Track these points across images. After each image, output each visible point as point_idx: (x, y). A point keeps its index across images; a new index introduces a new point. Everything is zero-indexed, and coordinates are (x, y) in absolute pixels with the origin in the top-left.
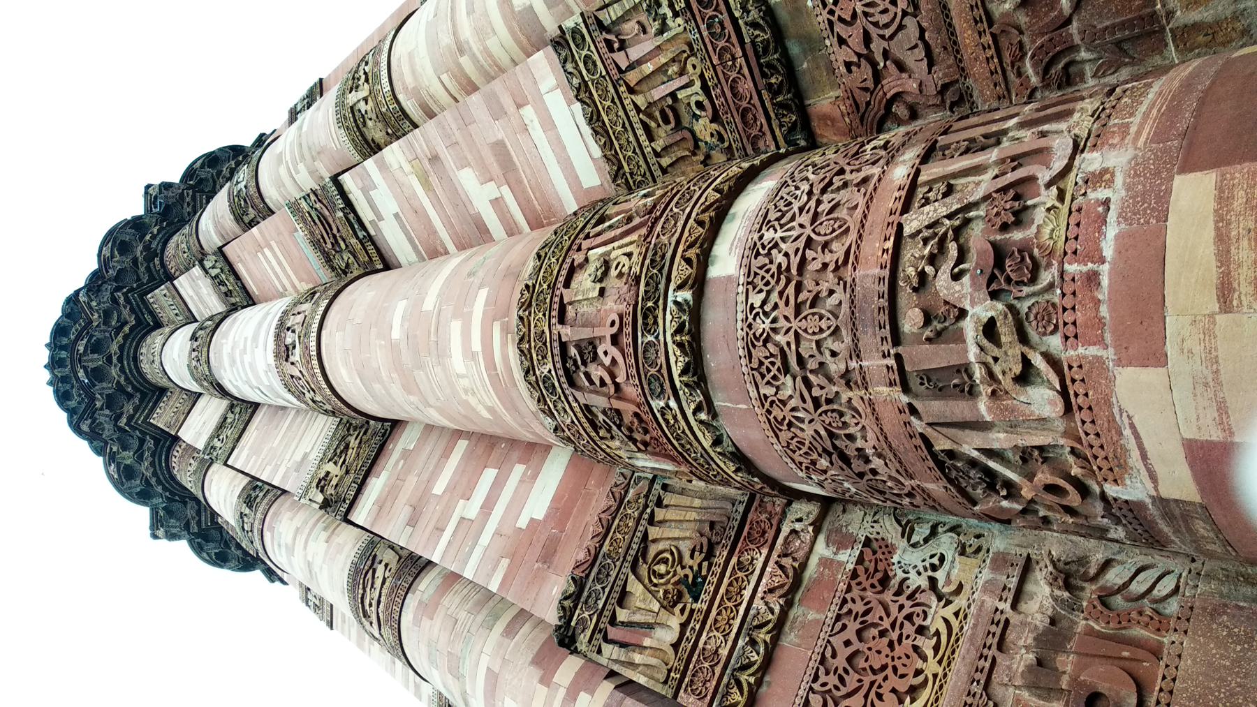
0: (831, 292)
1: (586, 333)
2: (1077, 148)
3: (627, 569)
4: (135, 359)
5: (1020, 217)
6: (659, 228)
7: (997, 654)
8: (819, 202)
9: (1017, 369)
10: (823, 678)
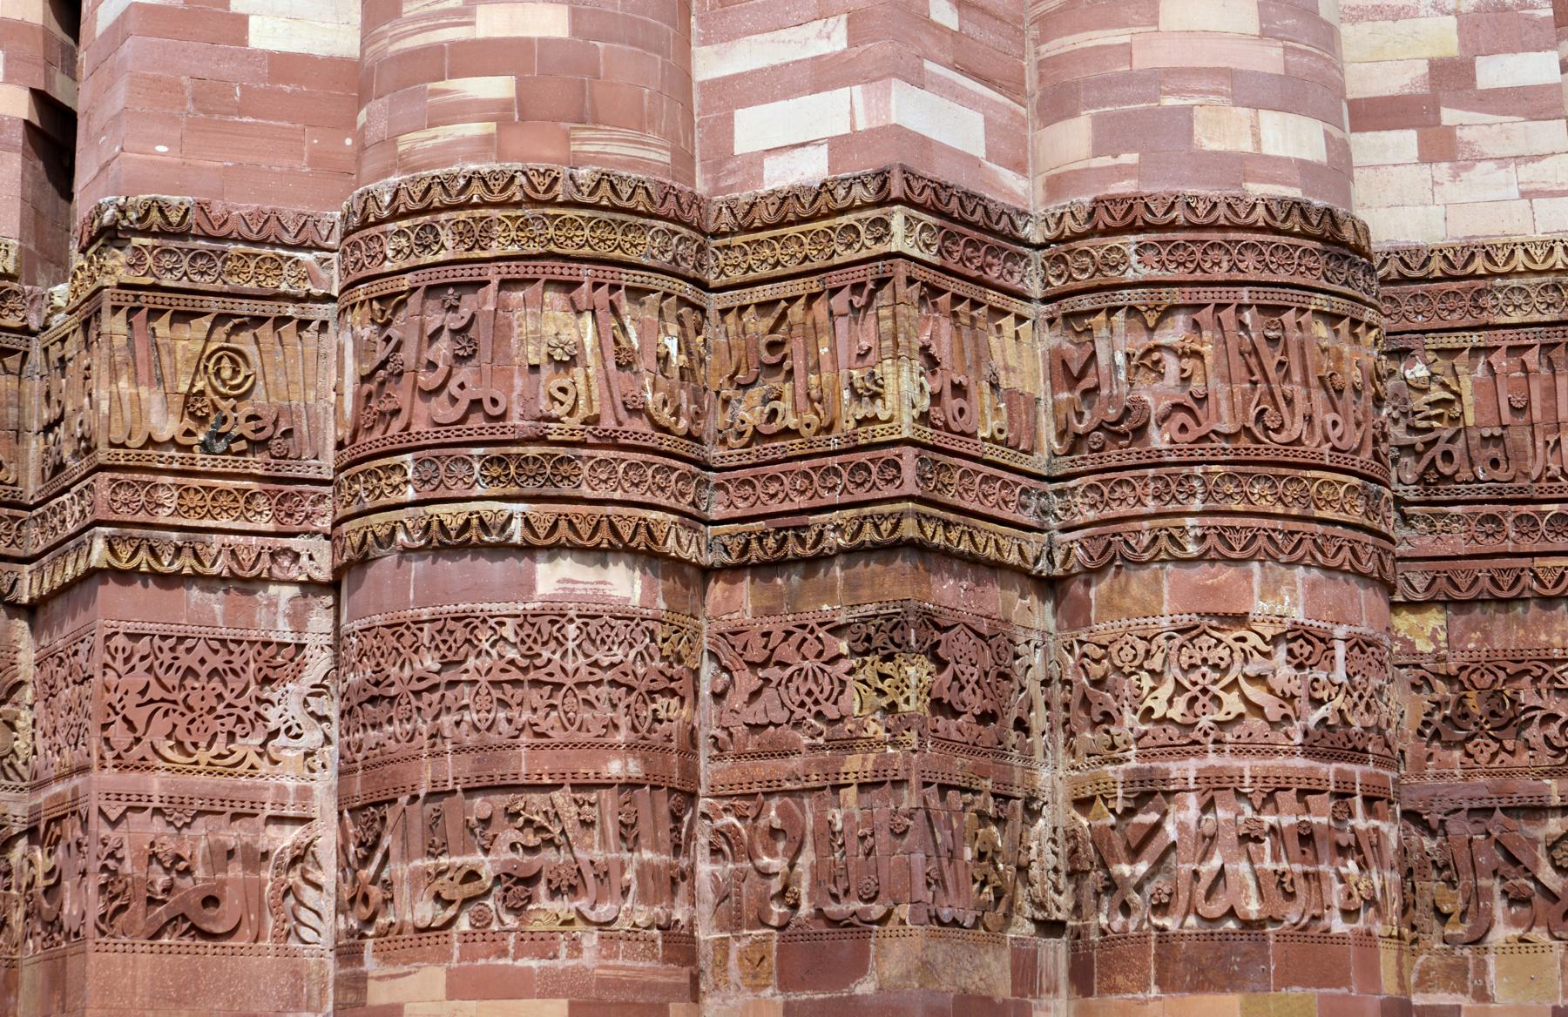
0: (510, 721)
3: (215, 306)
5: (555, 893)
6: (601, 454)
7: (228, 815)
8: (598, 683)
9: (445, 895)
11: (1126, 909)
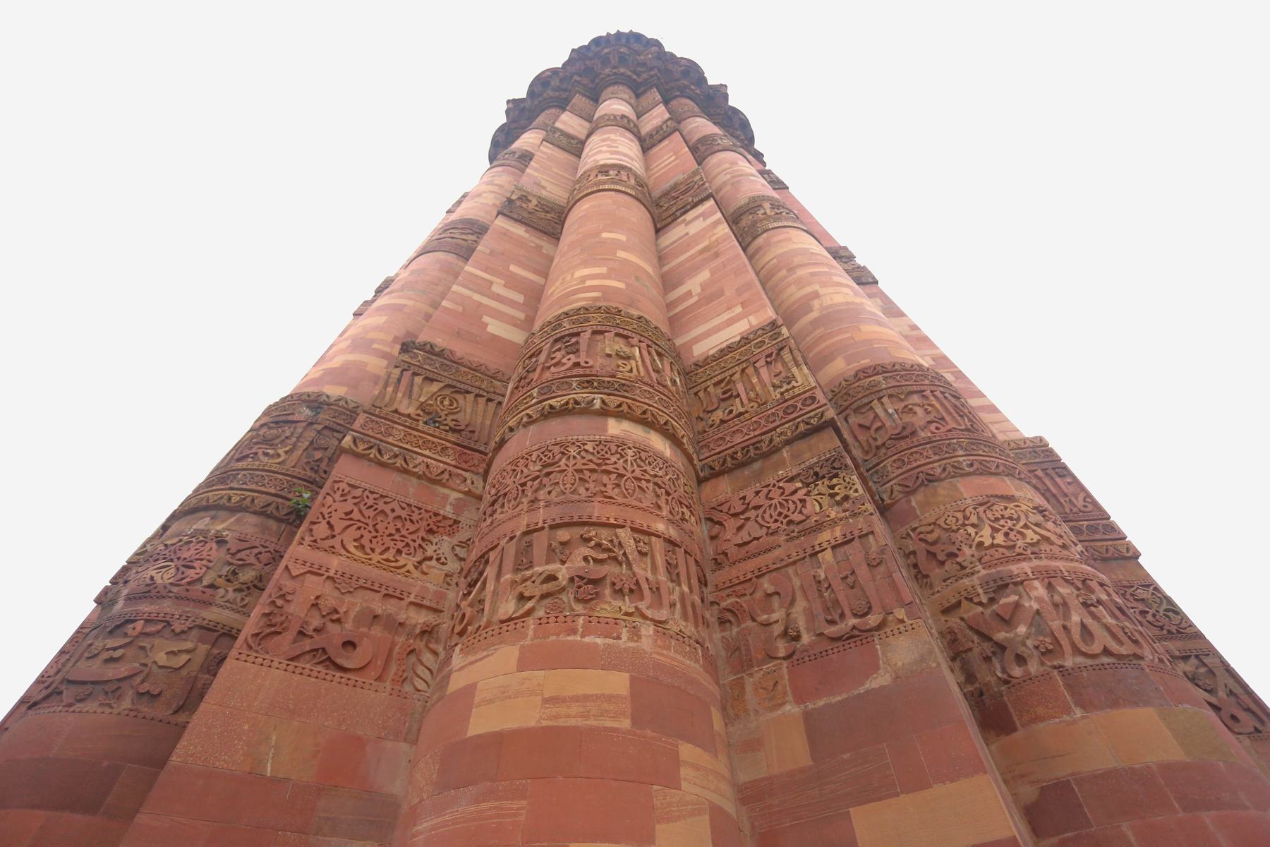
0: (587, 489)
1: (583, 346)
2: (657, 623)
3: (447, 381)
4: (615, 83)
5: (619, 592)
8: (648, 481)
9: (527, 594)
10: (372, 496)
11: (1021, 660)
